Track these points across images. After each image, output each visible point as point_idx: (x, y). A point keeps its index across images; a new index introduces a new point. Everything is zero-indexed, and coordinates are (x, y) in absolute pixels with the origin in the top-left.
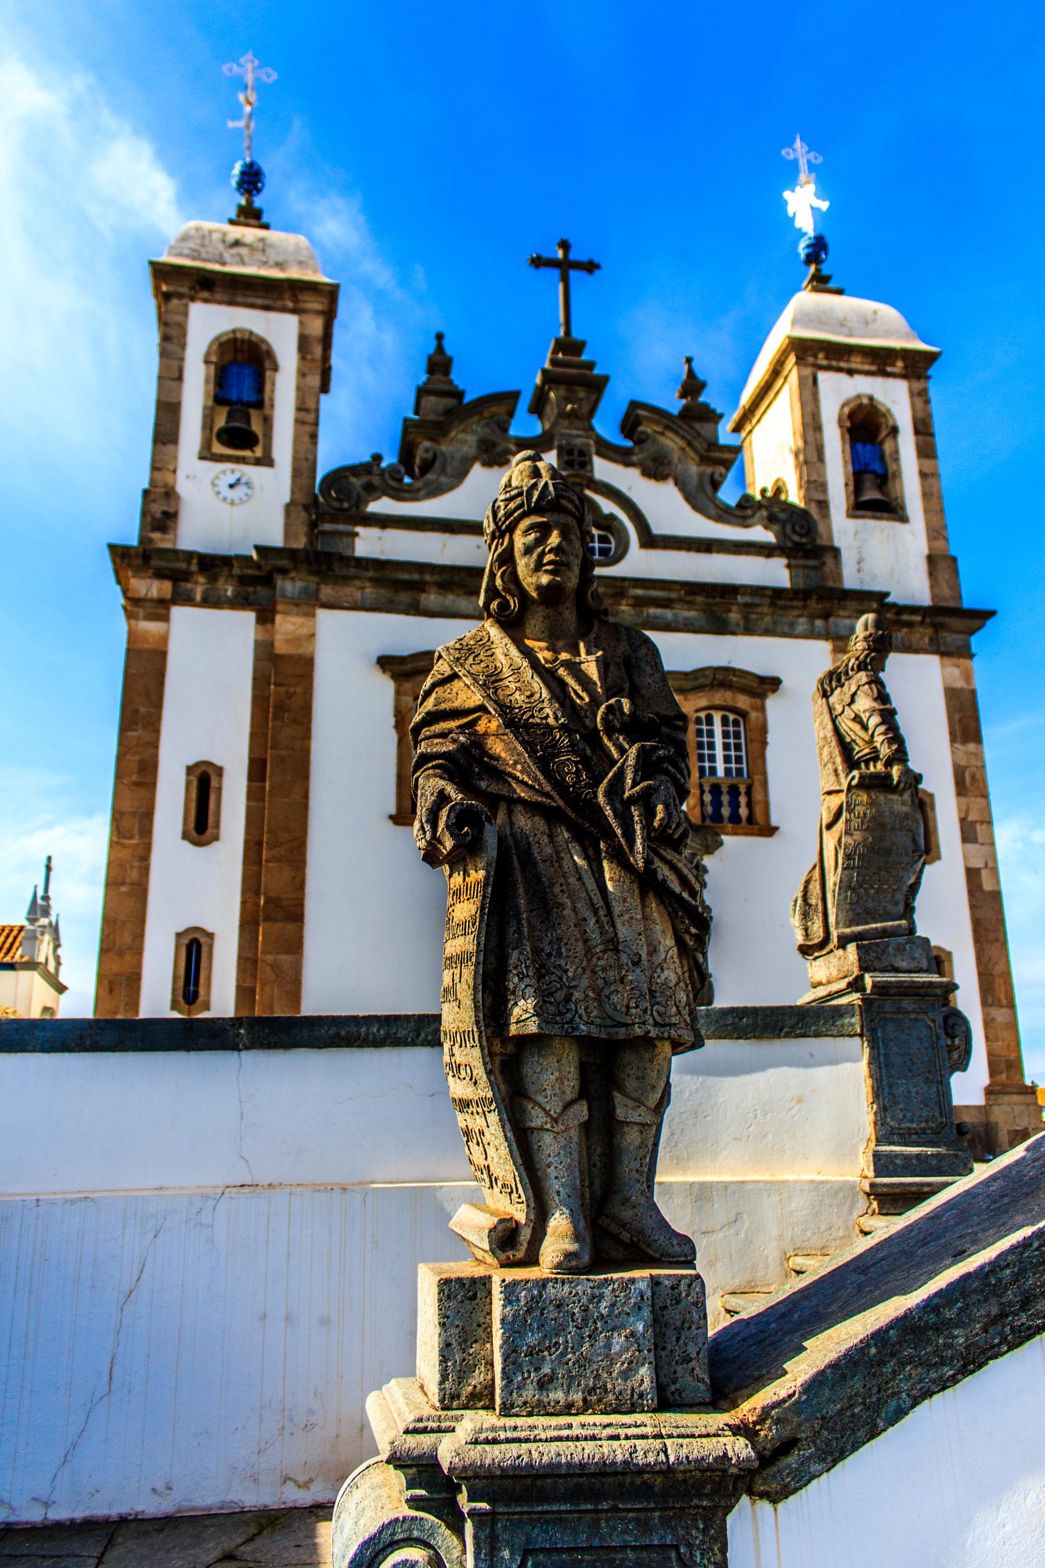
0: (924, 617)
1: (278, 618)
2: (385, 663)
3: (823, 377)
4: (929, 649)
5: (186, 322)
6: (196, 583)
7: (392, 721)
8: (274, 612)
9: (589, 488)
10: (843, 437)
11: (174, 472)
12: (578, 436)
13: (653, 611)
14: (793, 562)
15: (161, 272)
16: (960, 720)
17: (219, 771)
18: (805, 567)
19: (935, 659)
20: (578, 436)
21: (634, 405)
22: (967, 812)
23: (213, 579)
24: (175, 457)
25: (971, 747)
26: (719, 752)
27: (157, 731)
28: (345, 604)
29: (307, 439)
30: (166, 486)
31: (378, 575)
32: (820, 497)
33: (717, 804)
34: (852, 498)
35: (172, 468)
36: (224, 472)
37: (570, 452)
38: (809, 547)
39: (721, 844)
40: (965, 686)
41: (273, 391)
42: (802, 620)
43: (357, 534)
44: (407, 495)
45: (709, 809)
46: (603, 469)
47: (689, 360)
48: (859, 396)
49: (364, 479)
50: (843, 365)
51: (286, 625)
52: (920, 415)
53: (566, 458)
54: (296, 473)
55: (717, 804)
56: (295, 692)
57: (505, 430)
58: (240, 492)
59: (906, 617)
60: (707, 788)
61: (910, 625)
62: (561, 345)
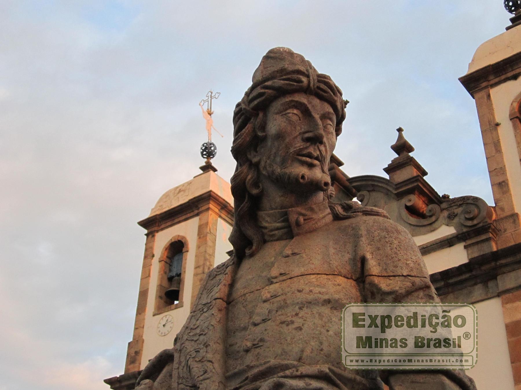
11: (143, 327)
14: (469, 242)
15: (144, 224)
18: (477, 243)
32: (501, 180)
35: (142, 326)
38: (481, 225)
41: (186, 263)
42: (476, 287)
47: (400, 130)
50: (510, 74)
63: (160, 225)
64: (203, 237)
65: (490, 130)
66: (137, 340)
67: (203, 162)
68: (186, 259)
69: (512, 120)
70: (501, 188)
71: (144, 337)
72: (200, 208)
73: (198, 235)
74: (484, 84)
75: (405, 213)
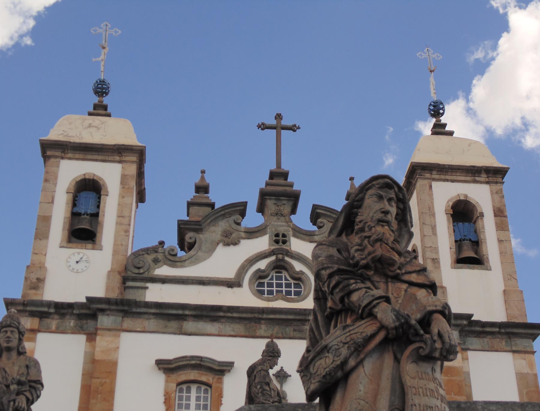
0: (500, 328)
1: (98, 338)
2: (159, 363)
3: (435, 184)
4: (505, 349)
5: (58, 171)
6: (53, 319)
7: (163, 399)
8: (96, 334)
9: (288, 256)
10: (448, 220)
11: (45, 255)
12: (282, 226)
16: (527, 393)
20: (282, 226)
21: (315, 207)
23: (63, 316)
24: (46, 247)
28: (138, 329)
29: (123, 233)
30: (40, 263)
31: (157, 311)
34: (454, 256)
35: (44, 253)
36: (74, 254)
37: (277, 235)
40: (530, 372)
41: (105, 207)
43: (147, 288)
44: (178, 264)
48: (458, 195)
49: (153, 256)
50: (448, 177)
52: (498, 205)
53: (274, 238)
54: (115, 252)
56: (105, 382)
57: (239, 224)
59: (488, 329)
61: (492, 333)
62: (273, 175)
63: (66, 152)
64: (128, 188)
65: (430, 215)
66: (40, 267)
67: (106, 100)
68: (105, 203)
69: (447, 214)
70: (434, 263)
71: (47, 265)
72: (124, 157)
73: (121, 183)
74: (428, 175)
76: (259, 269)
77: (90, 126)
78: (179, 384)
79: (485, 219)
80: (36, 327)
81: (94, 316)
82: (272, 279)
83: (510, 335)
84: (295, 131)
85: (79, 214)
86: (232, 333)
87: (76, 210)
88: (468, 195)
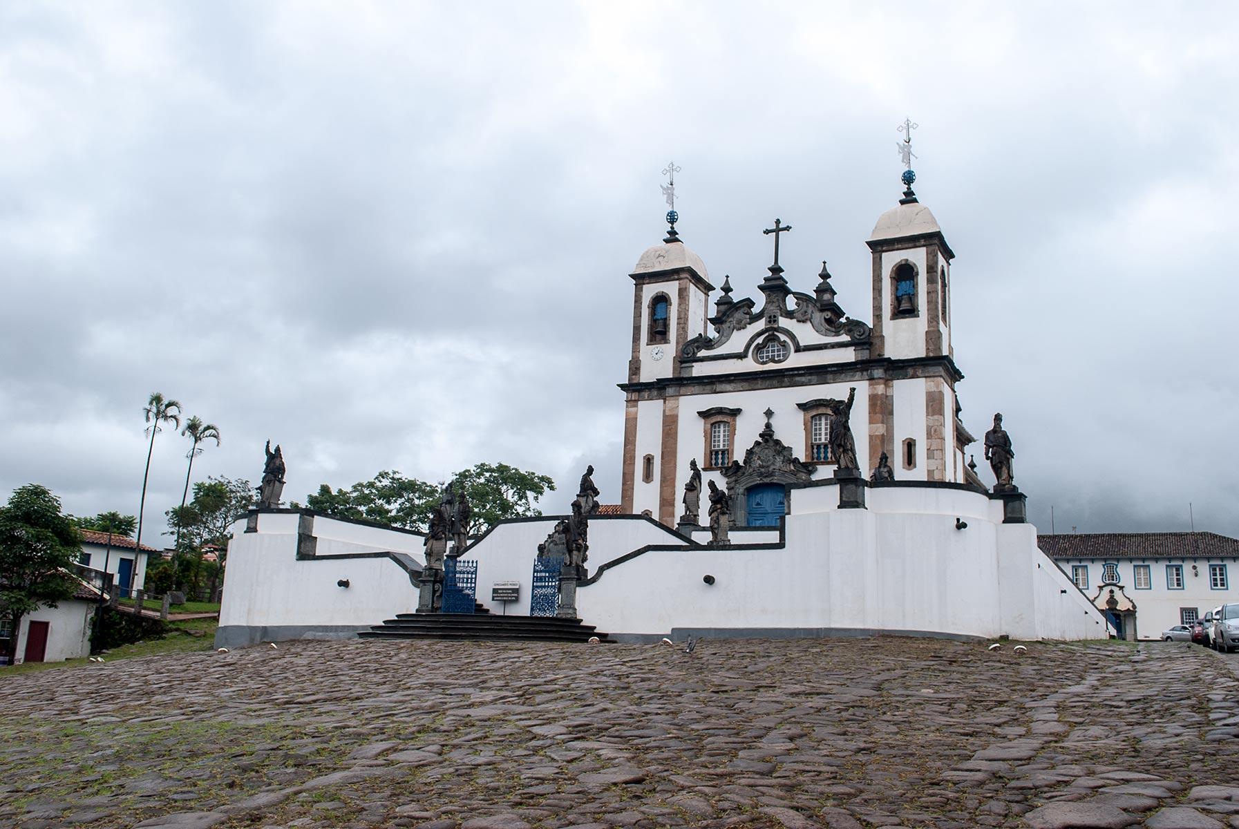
1: (667, 402)
3: (884, 254)
13: (798, 379)
16: (932, 405)
17: (653, 457)
19: (924, 379)
22: (931, 445)
23: (650, 390)
25: (936, 417)
26: (823, 432)
27: (635, 445)
33: (818, 453)
37: (770, 317)
38: (864, 340)
39: (816, 470)
42: (858, 373)
43: (693, 366)
44: (710, 348)
45: (816, 455)
46: (783, 322)
47: (825, 263)
48: (901, 261)
51: (670, 403)
52: (931, 263)
53: (768, 320)
54: (677, 343)
55: (818, 453)
58: (659, 355)
60: (815, 447)
75: (823, 321)
76: (758, 344)
77: (659, 256)
78: (712, 424)
79: (919, 277)
80: (637, 399)
81: (664, 388)
82: (768, 347)
83: (925, 365)
84: (788, 230)
85: (658, 319)
86: (741, 389)
87: (655, 317)
88: (909, 259)
